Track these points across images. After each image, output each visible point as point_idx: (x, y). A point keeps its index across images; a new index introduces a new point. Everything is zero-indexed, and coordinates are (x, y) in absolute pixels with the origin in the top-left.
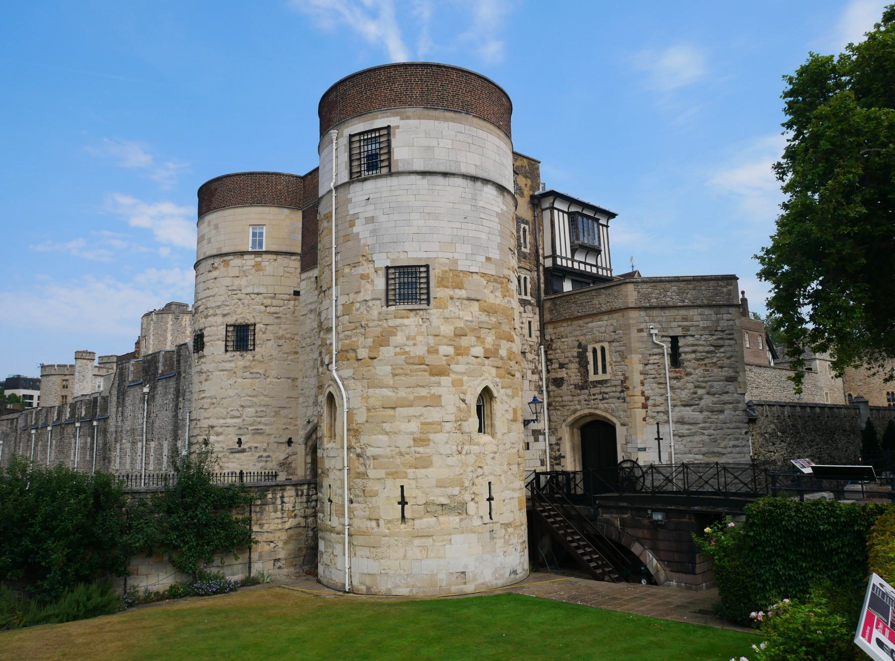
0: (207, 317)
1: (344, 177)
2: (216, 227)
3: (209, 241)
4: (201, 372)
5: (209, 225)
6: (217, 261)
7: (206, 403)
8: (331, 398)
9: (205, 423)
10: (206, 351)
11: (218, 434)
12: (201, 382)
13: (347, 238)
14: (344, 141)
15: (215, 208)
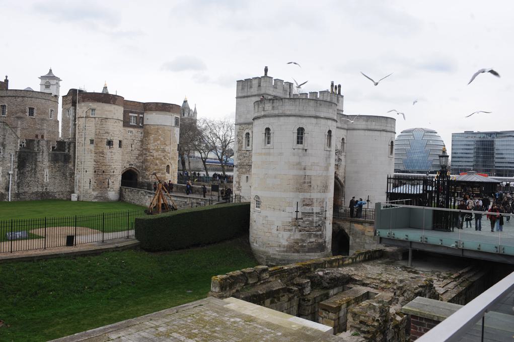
0: (114, 136)
1: (174, 125)
2: (117, 110)
3: (115, 114)
4: (112, 152)
5: (114, 108)
6: (117, 121)
7: (114, 161)
8: (168, 166)
9: (113, 167)
10: (114, 146)
11: (117, 170)
12: (112, 155)
13: (174, 137)
14: (174, 117)
15: (117, 105)
